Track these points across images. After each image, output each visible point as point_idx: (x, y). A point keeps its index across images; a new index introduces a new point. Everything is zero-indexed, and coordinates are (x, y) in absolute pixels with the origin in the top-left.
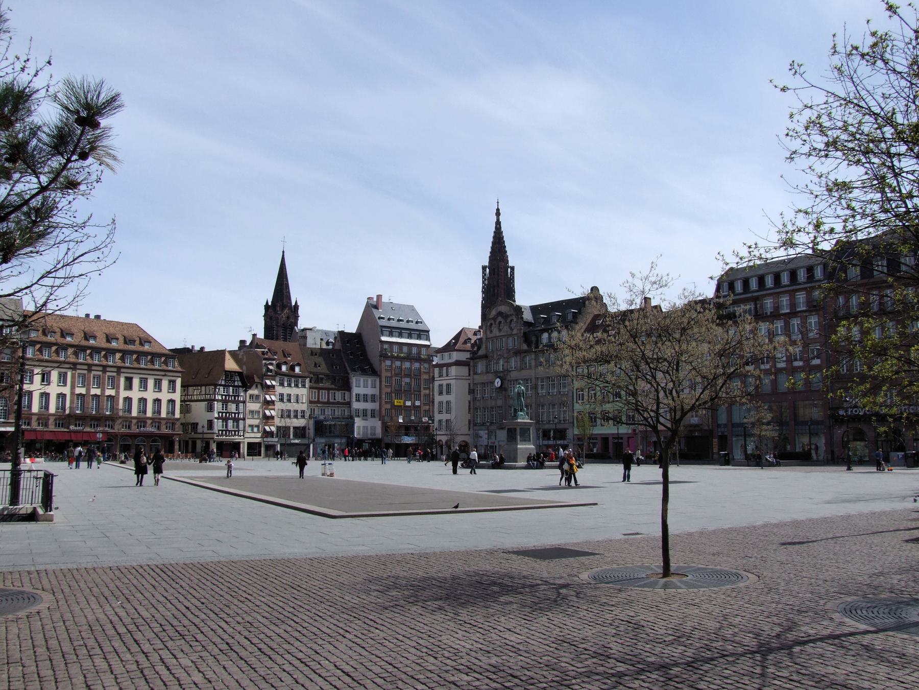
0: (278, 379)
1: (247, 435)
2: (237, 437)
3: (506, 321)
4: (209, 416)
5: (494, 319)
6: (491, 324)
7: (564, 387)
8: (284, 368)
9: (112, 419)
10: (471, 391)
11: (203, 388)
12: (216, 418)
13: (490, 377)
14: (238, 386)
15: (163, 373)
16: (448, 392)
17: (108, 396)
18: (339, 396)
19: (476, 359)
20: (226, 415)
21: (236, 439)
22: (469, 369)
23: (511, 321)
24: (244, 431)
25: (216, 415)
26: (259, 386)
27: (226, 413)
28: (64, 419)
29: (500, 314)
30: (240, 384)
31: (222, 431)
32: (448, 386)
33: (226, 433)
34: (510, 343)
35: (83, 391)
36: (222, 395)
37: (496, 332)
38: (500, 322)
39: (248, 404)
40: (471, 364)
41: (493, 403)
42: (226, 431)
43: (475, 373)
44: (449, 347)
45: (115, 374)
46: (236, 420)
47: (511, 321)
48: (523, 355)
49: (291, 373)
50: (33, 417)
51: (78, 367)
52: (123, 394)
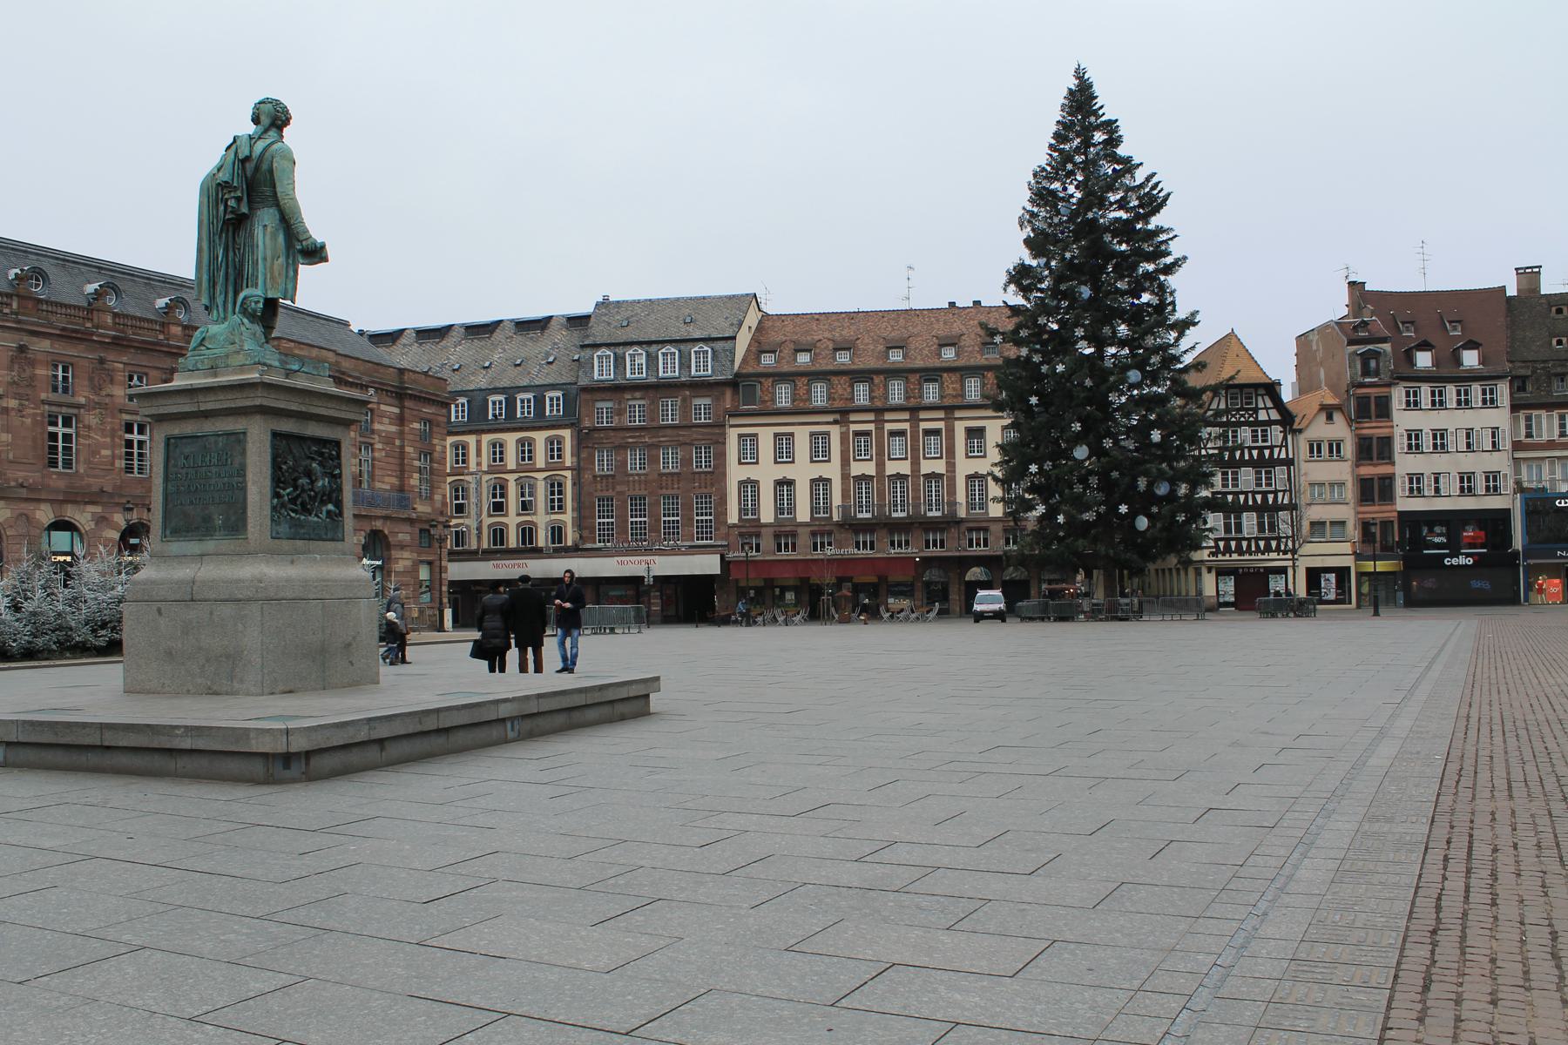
2: (1273, 555)
8: (1424, 360)
9: (950, 523)
14: (1270, 423)
17: (927, 476)
21: (1274, 559)
27: (1236, 494)
28: (821, 530)
30: (1275, 415)
33: (1239, 547)
35: (869, 469)
39: (1304, 467)
42: (1239, 541)
45: (940, 425)
50: (763, 530)
51: (853, 417)
52: (965, 467)
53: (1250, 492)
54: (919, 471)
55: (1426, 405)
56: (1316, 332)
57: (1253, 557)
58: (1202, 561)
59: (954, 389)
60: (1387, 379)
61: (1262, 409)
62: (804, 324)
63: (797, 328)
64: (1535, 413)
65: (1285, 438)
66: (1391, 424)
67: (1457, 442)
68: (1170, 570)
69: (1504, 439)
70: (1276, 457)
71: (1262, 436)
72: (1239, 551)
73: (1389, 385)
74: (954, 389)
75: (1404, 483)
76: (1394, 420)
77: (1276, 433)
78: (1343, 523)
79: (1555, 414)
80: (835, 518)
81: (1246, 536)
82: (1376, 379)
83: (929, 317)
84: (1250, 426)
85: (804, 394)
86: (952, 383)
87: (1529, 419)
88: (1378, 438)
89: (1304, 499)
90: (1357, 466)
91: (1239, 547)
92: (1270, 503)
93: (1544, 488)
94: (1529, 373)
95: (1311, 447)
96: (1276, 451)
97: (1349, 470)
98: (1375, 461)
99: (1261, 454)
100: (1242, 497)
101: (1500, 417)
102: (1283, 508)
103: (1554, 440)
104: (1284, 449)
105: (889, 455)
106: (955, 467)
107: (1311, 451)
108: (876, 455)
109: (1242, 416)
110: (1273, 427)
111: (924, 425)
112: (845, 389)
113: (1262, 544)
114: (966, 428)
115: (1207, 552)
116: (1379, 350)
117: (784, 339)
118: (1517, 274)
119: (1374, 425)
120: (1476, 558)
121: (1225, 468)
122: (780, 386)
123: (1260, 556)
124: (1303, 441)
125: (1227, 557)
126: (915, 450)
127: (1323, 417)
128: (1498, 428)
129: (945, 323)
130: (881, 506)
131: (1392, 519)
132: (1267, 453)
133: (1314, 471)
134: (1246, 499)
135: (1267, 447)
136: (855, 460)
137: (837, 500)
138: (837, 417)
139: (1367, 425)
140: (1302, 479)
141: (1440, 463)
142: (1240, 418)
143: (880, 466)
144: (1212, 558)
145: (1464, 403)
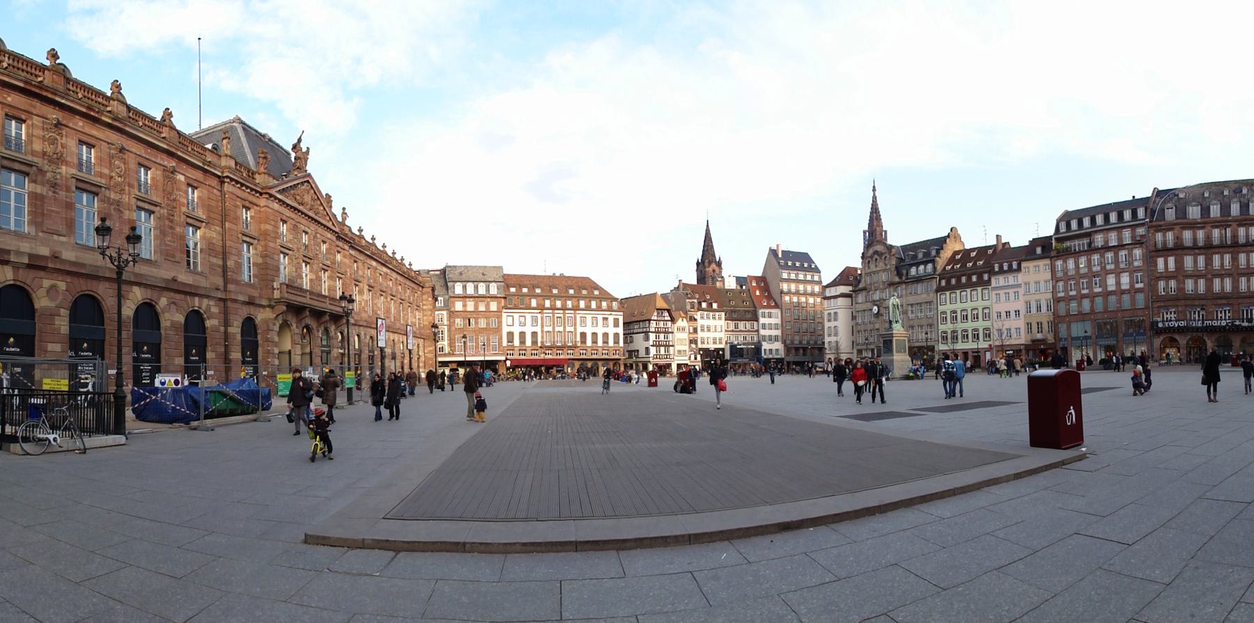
0: (699, 313)
1: (676, 358)
3: (881, 258)
4: (646, 344)
5: (871, 257)
6: (869, 262)
7: (930, 311)
8: (704, 305)
10: (854, 318)
11: (641, 323)
13: (869, 305)
14: (668, 321)
15: (609, 313)
16: (835, 320)
18: (748, 324)
19: (857, 291)
22: (852, 300)
23: (886, 257)
24: (674, 355)
25: (651, 343)
26: (684, 319)
27: (659, 341)
29: (876, 252)
30: (669, 318)
32: (836, 313)
33: (660, 358)
34: (884, 277)
37: (873, 268)
38: (876, 259)
40: (853, 296)
41: (872, 327)
43: (856, 303)
44: (834, 283)
46: (667, 346)
47: (886, 257)
48: (895, 286)
49: (710, 309)
67: (712, 329)
72: (660, 358)
78: (685, 351)
79: (734, 322)
89: (676, 343)
127: (681, 319)
133: (678, 335)
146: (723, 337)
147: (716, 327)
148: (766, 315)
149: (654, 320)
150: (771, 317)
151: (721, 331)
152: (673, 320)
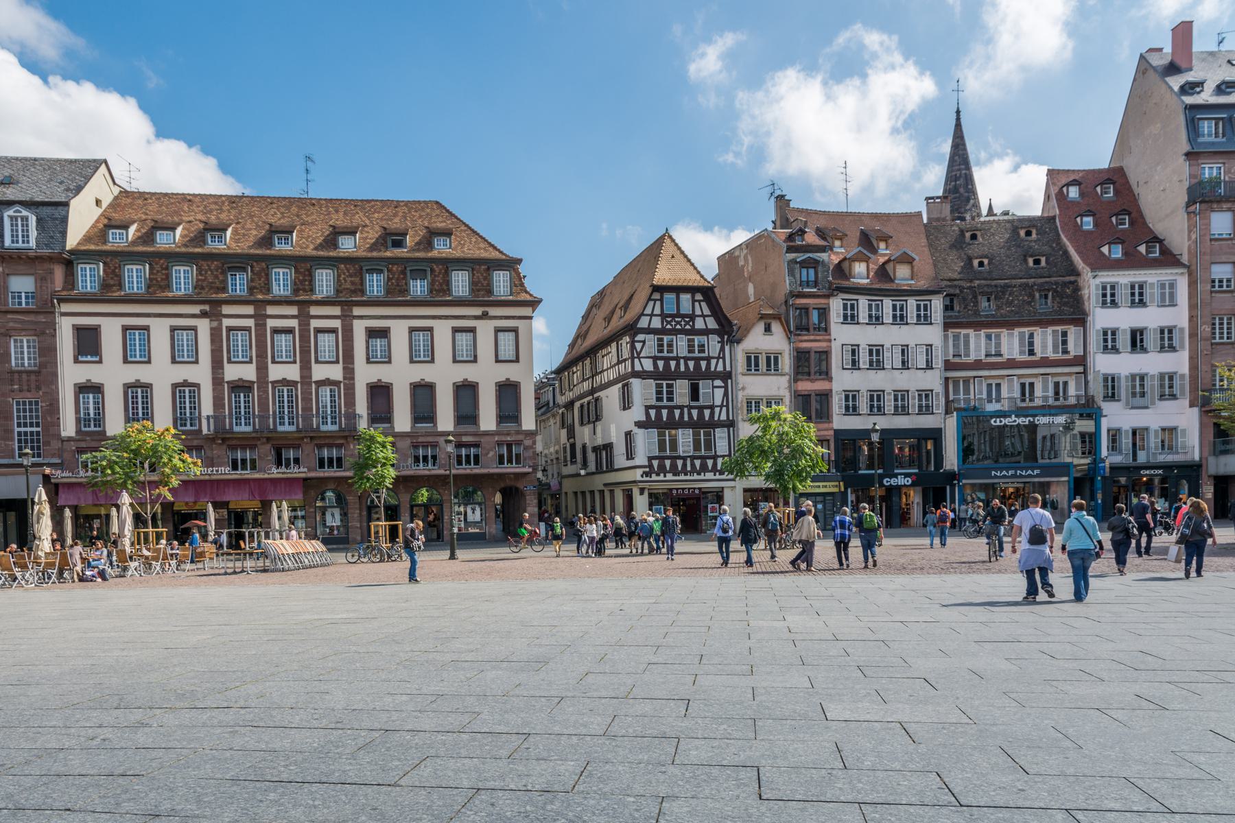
2: (710, 476)
12: (639, 424)
14: (706, 332)
15: (478, 311)
18: (1045, 341)
20: (671, 414)
21: (709, 481)
26: (776, 327)
30: (712, 324)
31: (661, 459)
33: (674, 466)
35: (248, 372)
36: (655, 359)
39: (743, 380)
42: (674, 459)
46: (704, 426)
51: (226, 310)
52: (365, 374)
53: (687, 406)
54: (311, 378)
55: (864, 318)
56: (744, 246)
57: (688, 477)
58: (634, 482)
59: (353, 283)
60: (825, 292)
61: (698, 316)
62: (172, 203)
63: (164, 207)
64: (964, 331)
65: (722, 349)
66: (827, 337)
68: (592, 492)
69: (936, 356)
70: (713, 369)
71: (694, 346)
73: (828, 296)
74: (353, 283)
75: (840, 400)
76: (832, 333)
77: (713, 345)
79: (983, 332)
80: (205, 431)
81: (681, 454)
82: (815, 290)
83: (327, 206)
84: (686, 335)
85: (162, 279)
86: (351, 276)
87: (956, 337)
88: (816, 352)
90: (796, 381)
91: (674, 466)
92: (707, 419)
93: (975, 407)
94: (957, 291)
95: (749, 359)
96: (713, 362)
97: (787, 385)
98: (812, 377)
99: (697, 366)
100: (677, 412)
101: (932, 334)
102: (721, 424)
103: (981, 360)
104: (721, 360)
105: (273, 357)
106: (354, 374)
107: (749, 364)
108: (257, 357)
109: (678, 323)
110: (710, 336)
111: (315, 323)
112: (216, 277)
113: (698, 463)
114: (366, 328)
115: (639, 472)
116: (818, 259)
117: (144, 217)
118: (928, 203)
119: (812, 337)
120: (914, 477)
121: (660, 379)
122: (130, 267)
123: (696, 477)
124: (740, 351)
125: (661, 477)
126: (305, 351)
127: (760, 327)
128: (931, 346)
129: (345, 214)
130: (264, 417)
131: (828, 438)
132: (703, 364)
134: (682, 414)
135: (703, 359)
136: (230, 361)
137: (207, 408)
138: (207, 308)
139: (806, 338)
140: (740, 395)
141: (877, 380)
142: (675, 325)
143: (262, 370)
144: (645, 479)
145: (900, 319)
146: (938, 387)
147: (904, 349)
148: (1123, 295)
149: (649, 331)
150: (1142, 303)
151: (929, 366)
152: (728, 331)
